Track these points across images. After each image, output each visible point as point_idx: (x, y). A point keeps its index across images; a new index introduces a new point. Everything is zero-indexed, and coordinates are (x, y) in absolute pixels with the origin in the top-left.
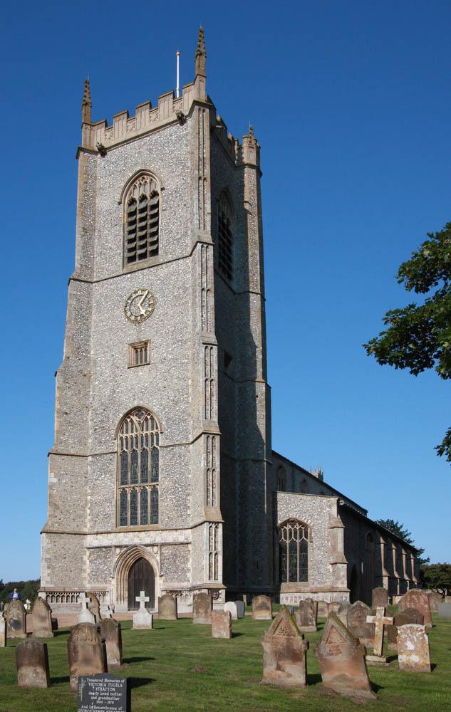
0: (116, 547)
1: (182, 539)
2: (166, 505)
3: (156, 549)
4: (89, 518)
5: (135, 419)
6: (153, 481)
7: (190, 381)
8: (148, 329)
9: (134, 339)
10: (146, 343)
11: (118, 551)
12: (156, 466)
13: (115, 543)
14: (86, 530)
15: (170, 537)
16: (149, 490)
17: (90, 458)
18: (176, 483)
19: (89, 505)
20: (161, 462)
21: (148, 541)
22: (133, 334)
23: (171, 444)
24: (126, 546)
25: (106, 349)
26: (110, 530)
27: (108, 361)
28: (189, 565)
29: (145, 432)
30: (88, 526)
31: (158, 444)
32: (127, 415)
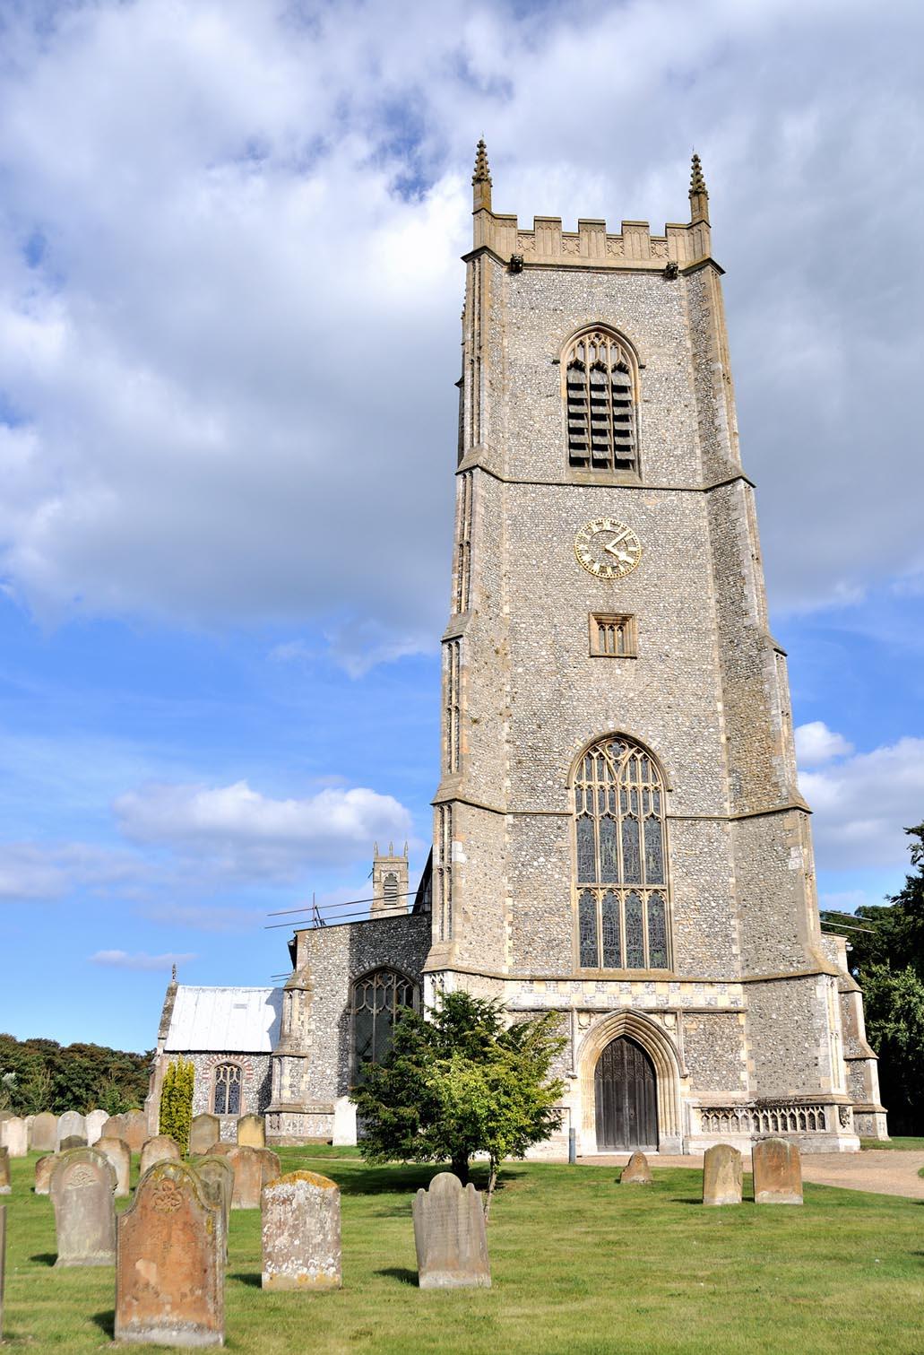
0: (581, 1011)
1: (724, 1002)
2: (682, 932)
3: (669, 1019)
4: (510, 943)
5: (607, 753)
6: (651, 881)
7: (720, 706)
8: (627, 594)
9: (600, 606)
10: (625, 618)
11: (584, 1019)
12: (657, 856)
13: (576, 1001)
14: (505, 971)
15: (700, 997)
16: (645, 897)
17: (509, 819)
18: (704, 890)
19: (510, 917)
20: (671, 847)
21: (651, 1002)
23: (688, 814)
24: (604, 1011)
26: (562, 973)
27: (544, 634)
28: (743, 1055)
29: (629, 784)
30: (510, 961)
31: (657, 810)
32: (594, 745)
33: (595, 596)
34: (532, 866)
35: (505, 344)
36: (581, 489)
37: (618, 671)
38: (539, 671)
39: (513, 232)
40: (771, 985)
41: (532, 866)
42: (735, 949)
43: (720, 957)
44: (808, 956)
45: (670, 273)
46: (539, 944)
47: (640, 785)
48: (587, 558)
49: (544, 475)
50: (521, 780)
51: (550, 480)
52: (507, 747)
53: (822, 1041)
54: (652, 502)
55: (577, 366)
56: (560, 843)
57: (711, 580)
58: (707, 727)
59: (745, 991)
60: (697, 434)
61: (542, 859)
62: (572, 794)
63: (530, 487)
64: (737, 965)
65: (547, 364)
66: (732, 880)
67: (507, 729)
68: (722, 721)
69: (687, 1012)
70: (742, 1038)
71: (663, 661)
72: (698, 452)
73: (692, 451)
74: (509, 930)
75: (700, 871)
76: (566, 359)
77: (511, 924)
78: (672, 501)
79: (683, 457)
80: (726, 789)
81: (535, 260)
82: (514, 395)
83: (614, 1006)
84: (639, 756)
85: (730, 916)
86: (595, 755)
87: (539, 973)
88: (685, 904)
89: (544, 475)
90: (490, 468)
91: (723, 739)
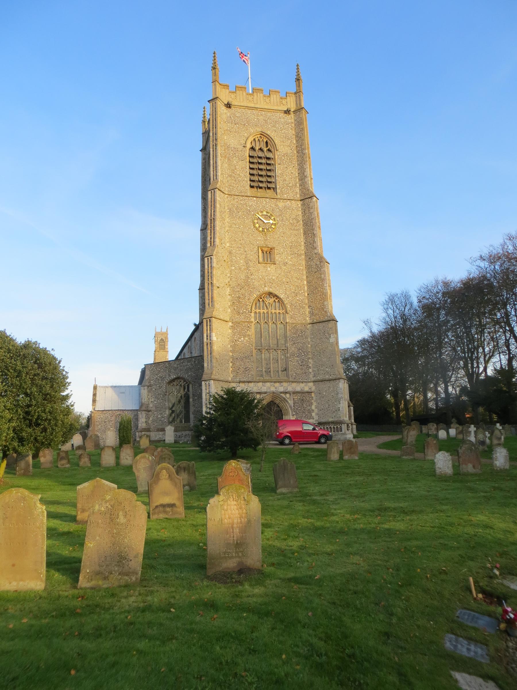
1: (306, 389)
3: (288, 395)
4: (231, 369)
7: (305, 282)
14: (230, 379)
15: (298, 387)
19: (231, 360)
21: (281, 389)
22: (260, 240)
24: (265, 393)
25: (240, 246)
26: (250, 380)
30: (232, 376)
33: (260, 240)
34: (239, 341)
35: (225, 138)
36: (255, 199)
37: (269, 269)
38: (240, 269)
39: (227, 91)
40: (323, 382)
41: (239, 341)
42: (310, 370)
43: (305, 373)
44: (337, 372)
45: (287, 112)
46: (242, 370)
47: (278, 311)
48: (257, 225)
49: (241, 192)
50: (234, 309)
51: (243, 194)
52: (229, 297)
53: (341, 402)
54: (281, 204)
55: (252, 149)
56: (249, 333)
57: (302, 235)
58: (301, 290)
59: (314, 385)
60: (297, 178)
61: (242, 339)
62: (253, 314)
63: (236, 197)
64: (311, 376)
65: (241, 147)
66: (309, 346)
67: (229, 291)
68: (306, 288)
69: (294, 393)
70: (313, 401)
71: (285, 265)
72: (298, 185)
73: (296, 185)
74: (231, 364)
75: (298, 342)
76: (249, 146)
77: (231, 362)
78: (288, 204)
79: (292, 187)
80: (307, 313)
81: (236, 104)
82: (229, 159)
83: (269, 391)
84: (277, 301)
85: (309, 358)
86: (261, 300)
87: (242, 380)
88: (293, 355)
89: (241, 192)
90: (221, 189)
91: (306, 295)
